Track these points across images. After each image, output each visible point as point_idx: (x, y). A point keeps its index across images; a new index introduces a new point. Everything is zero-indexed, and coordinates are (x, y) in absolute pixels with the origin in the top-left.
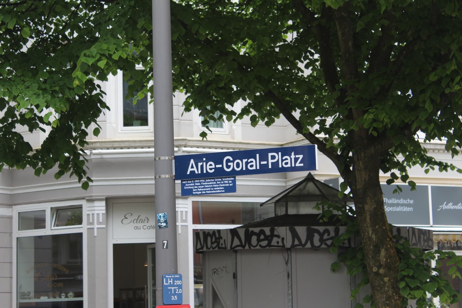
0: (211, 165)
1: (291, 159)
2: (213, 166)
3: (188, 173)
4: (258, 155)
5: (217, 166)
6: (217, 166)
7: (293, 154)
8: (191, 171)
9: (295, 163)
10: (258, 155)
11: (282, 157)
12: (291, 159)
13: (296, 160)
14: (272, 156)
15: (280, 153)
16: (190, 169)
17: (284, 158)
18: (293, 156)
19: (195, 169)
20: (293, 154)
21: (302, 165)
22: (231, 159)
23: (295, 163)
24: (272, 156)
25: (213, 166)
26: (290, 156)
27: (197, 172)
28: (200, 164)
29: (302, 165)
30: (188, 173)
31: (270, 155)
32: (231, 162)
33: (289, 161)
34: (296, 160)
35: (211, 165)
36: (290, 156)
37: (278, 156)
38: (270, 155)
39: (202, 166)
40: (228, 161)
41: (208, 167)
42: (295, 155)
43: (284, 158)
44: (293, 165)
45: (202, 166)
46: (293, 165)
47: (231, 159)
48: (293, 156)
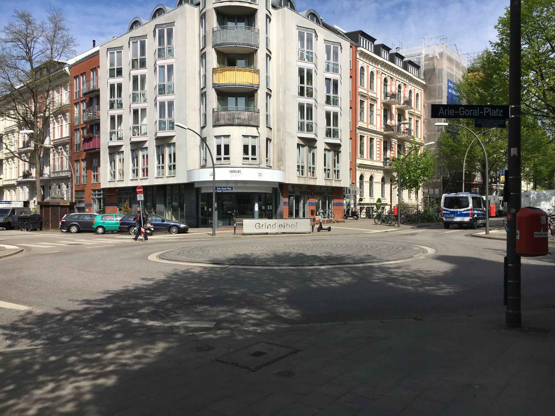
0: (452, 111)
1: (496, 112)
2: (454, 112)
3: (439, 114)
4: (478, 108)
5: (456, 112)
6: (456, 112)
7: (497, 109)
8: (441, 114)
9: (498, 114)
10: (478, 108)
11: (491, 110)
12: (496, 112)
13: (499, 112)
14: (486, 109)
15: (490, 108)
16: (440, 113)
17: (492, 111)
18: (497, 111)
19: (443, 113)
20: (497, 109)
21: (502, 115)
22: (464, 109)
23: (498, 114)
24: (486, 109)
25: (454, 112)
26: (496, 110)
27: (444, 115)
28: (446, 110)
29: (502, 115)
30: (439, 114)
31: (485, 108)
32: (463, 110)
33: (495, 113)
34: (499, 112)
35: (452, 111)
36: (496, 110)
37: (489, 110)
38: (485, 108)
39: (447, 111)
40: (462, 110)
41: (451, 112)
42: (498, 110)
43: (492, 111)
44: (497, 115)
45: (447, 111)
46: (497, 115)
47: (464, 109)
48: (497, 111)
